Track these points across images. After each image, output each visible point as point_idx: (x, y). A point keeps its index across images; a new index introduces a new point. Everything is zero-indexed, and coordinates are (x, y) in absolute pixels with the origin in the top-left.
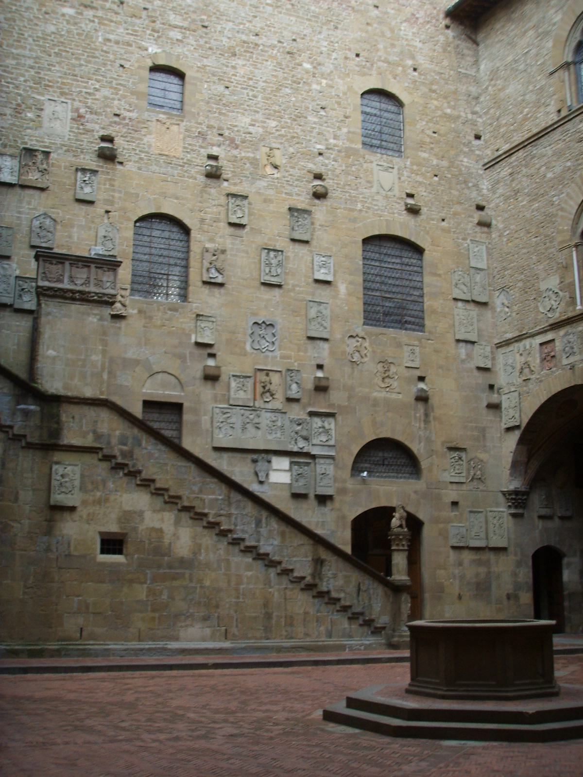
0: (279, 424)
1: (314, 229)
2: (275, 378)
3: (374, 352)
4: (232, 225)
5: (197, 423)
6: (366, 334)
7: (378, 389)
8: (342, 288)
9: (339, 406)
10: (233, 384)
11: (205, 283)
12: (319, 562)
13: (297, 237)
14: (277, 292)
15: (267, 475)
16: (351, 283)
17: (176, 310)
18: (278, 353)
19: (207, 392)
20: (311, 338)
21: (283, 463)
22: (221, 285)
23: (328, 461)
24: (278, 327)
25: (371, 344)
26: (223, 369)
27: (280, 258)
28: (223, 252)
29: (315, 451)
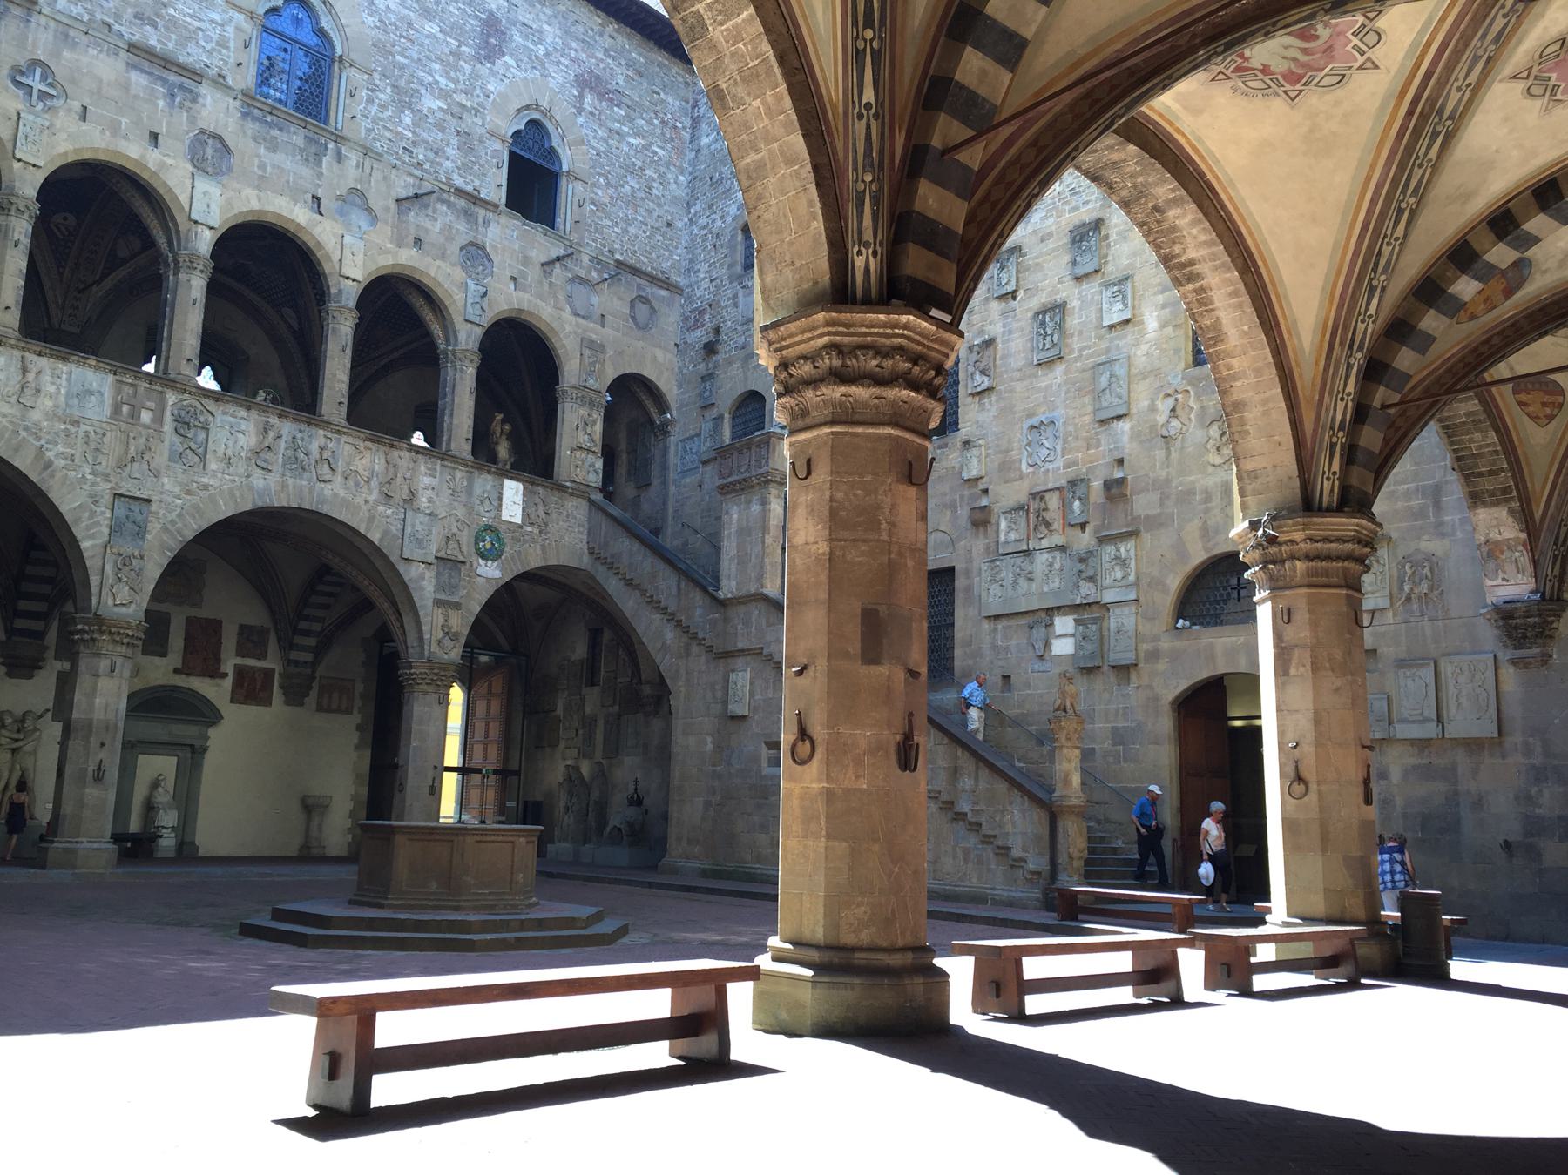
0: (1057, 566)
1: (1109, 246)
2: (1053, 501)
3: (1202, 408)
4: (1001, 297)
5: (968, 589)
6: (1190, 383)
7: (1211, 469)
8: (1151, 322)
9: (1147, 517)
10: (1003, 525)
11: (973, 395)
12: (955, 772)
13: (1080, 271)
14: (1060, 369)
15: (1047, 645)
16: (1164, 306)
17: (946, 445)
18: (1060, 462)
19: (978, 545)
20: (1103, 422)
21: (1064, 624)
22: (990, 389)
23: (1126, 610)
24: (1060, 423)
25: (1198, 397)
26: (996, 508)
27: (1057, 319)
28: (990, 343)
29: (1109, 597)
